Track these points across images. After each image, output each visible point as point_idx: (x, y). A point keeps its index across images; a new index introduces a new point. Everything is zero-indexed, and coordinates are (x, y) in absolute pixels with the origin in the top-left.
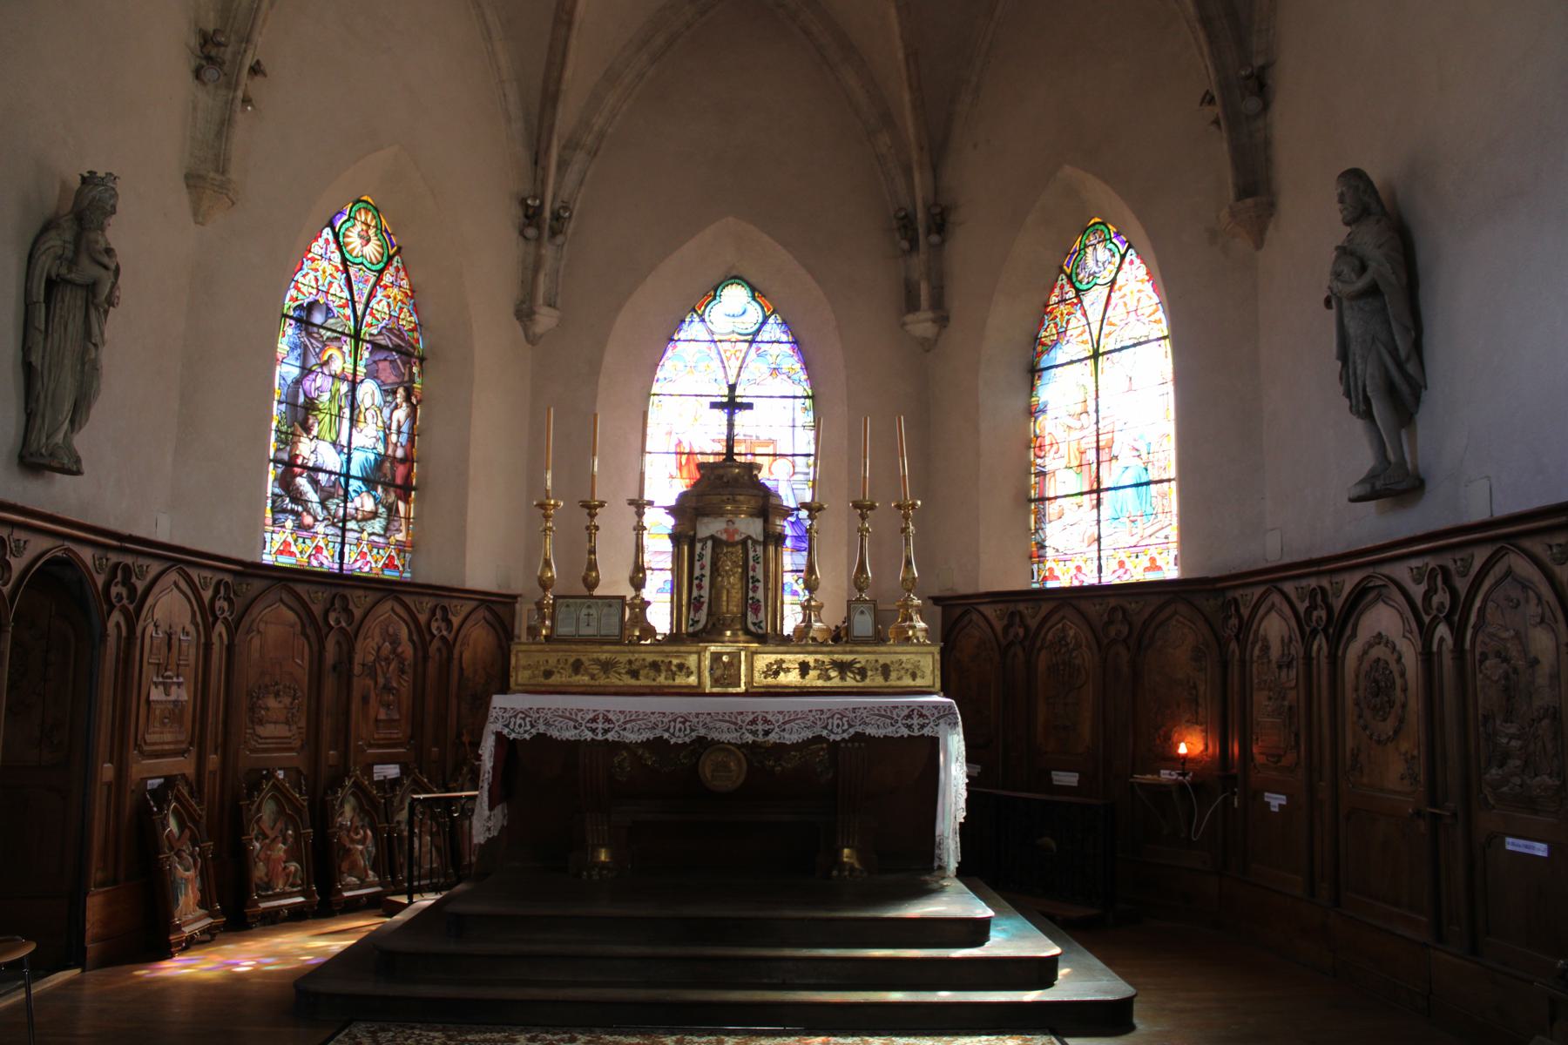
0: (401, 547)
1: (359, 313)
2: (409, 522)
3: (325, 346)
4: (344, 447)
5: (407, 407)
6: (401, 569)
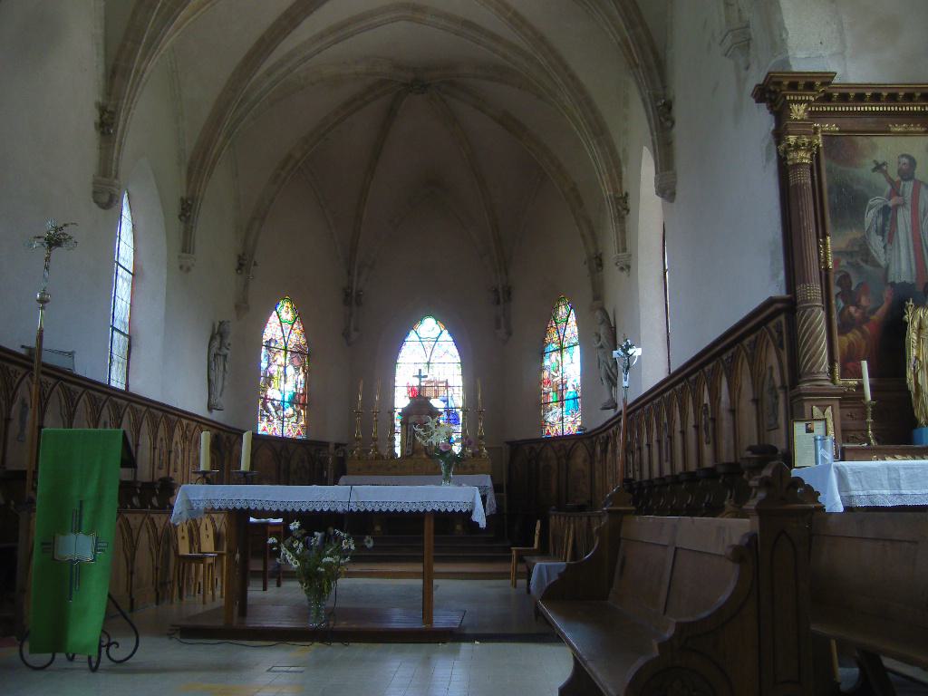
0: (302, 426)
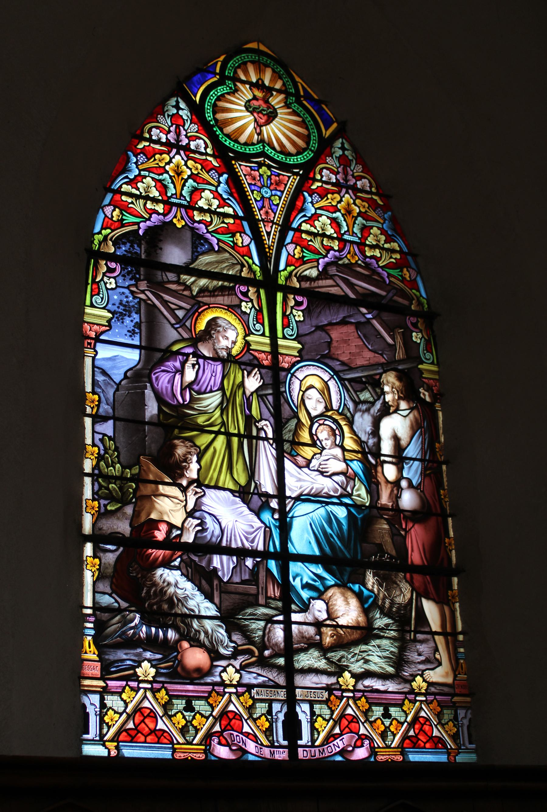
1: (270, 241)
2: (455, 640)
3: (200, 304)
4: (267, 495)
5: (411, 409)
6: (450, 744)
